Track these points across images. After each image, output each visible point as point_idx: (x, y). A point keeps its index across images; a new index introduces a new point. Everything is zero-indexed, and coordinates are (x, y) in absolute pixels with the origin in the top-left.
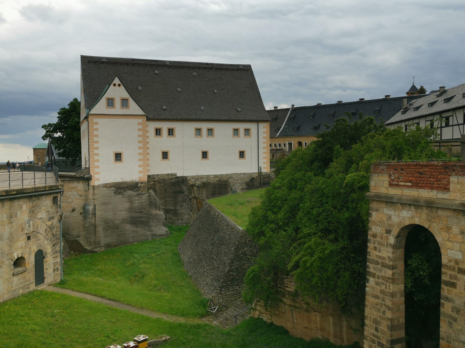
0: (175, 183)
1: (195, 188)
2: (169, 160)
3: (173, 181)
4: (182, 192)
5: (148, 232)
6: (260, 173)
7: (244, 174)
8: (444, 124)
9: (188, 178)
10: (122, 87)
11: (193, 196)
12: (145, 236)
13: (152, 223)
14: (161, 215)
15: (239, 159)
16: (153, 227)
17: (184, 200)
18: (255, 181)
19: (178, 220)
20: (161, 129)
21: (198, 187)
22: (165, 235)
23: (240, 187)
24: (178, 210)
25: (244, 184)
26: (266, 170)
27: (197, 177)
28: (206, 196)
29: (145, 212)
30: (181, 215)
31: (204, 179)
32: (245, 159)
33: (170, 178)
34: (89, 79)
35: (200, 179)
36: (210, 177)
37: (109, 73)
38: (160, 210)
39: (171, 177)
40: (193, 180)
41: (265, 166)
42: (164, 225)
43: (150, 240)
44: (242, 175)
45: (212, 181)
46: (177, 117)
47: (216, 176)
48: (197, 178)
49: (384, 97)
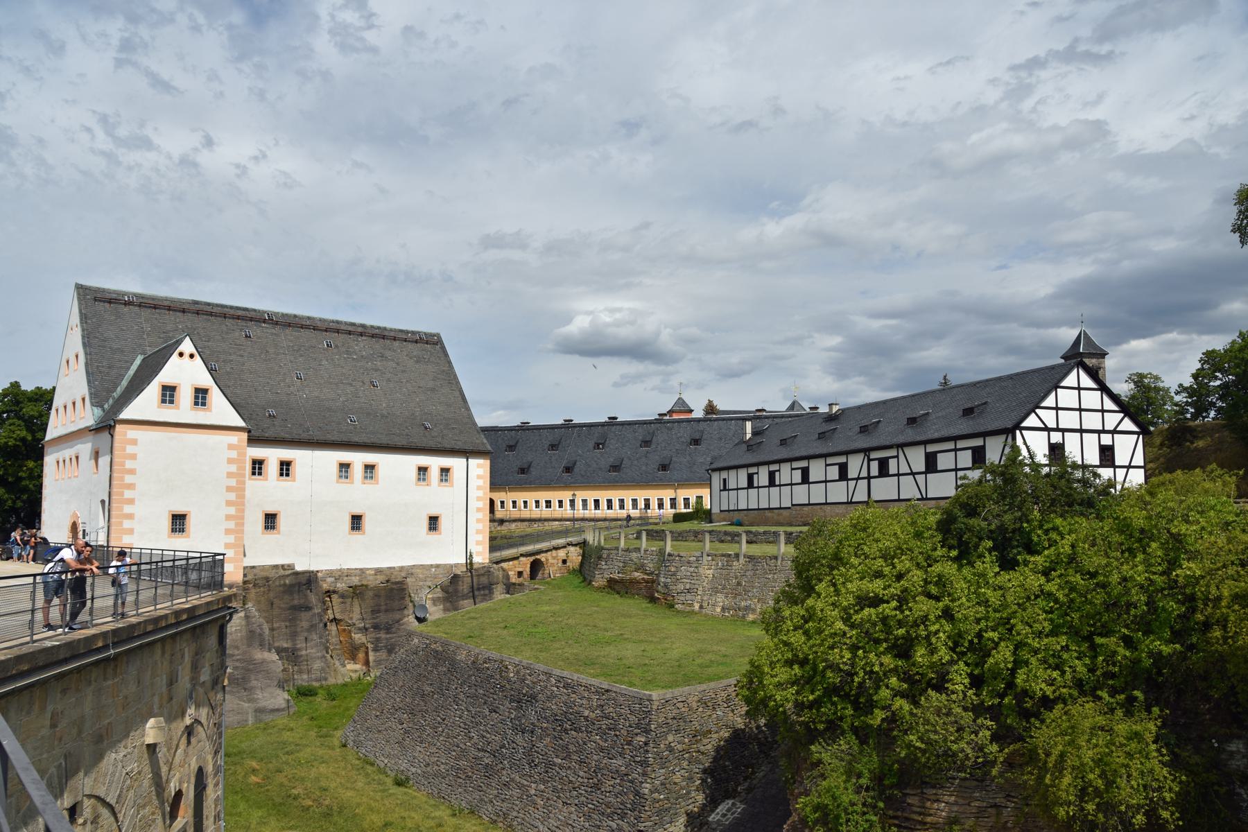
0: (292, 586)
1: (335, 597)
2: (279, 533)
3: (287, 582)
4: (308, 608)
5: (247, 705)
6: (470, 564)
7: (438, 566)
8: (875, 470)
9: (319, 574)
10: (198, 358)
11: (331, 617)
12: (238, 713)
13: (254, 683)
14: (274, 662)
15: (427, 534)
16: (258, 692)
17: (312, 627)
18: (460, 583)
19: (300, 672)
20: (291, 462)
21: (342, 596)
22: (283, 710)
23: (429, 596)
24: (299, 649)
25: (439, 589)
26: (481, 557)
27: (340, 573)
28: (359, 617)
29: (238, 655)
30: (307, 661)
31: (353, 578)
32: (440, 534)
33: (280, 574)
34: (97, 338)
35: (346, 578)
36: (368, 572)
37: (142, 328)
38: (270, 650)
39: (282, 572)
40: (330, 580)
41: (480, 548)
42: (279, 687)
43: (250, 722)
44: (433, 570)
45: (373, 581)
46: (300, 435)
47: (378, 571)
48: (340, 576)
49: (607, 420)
